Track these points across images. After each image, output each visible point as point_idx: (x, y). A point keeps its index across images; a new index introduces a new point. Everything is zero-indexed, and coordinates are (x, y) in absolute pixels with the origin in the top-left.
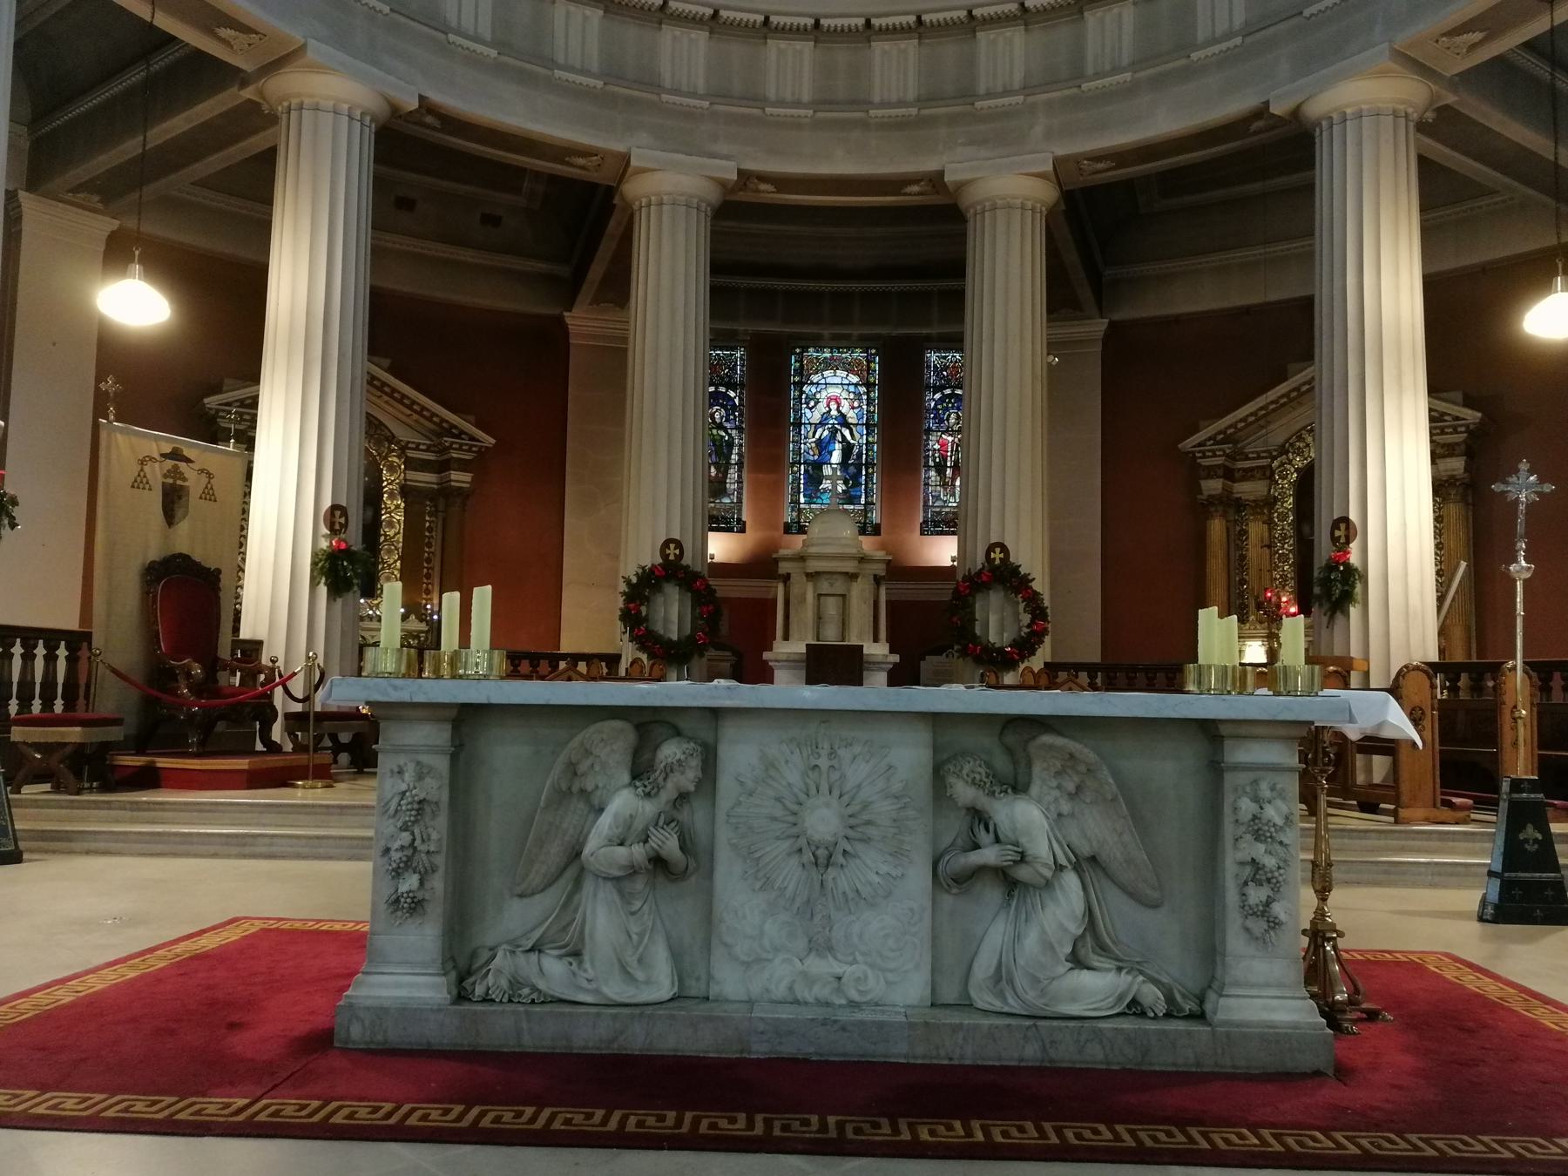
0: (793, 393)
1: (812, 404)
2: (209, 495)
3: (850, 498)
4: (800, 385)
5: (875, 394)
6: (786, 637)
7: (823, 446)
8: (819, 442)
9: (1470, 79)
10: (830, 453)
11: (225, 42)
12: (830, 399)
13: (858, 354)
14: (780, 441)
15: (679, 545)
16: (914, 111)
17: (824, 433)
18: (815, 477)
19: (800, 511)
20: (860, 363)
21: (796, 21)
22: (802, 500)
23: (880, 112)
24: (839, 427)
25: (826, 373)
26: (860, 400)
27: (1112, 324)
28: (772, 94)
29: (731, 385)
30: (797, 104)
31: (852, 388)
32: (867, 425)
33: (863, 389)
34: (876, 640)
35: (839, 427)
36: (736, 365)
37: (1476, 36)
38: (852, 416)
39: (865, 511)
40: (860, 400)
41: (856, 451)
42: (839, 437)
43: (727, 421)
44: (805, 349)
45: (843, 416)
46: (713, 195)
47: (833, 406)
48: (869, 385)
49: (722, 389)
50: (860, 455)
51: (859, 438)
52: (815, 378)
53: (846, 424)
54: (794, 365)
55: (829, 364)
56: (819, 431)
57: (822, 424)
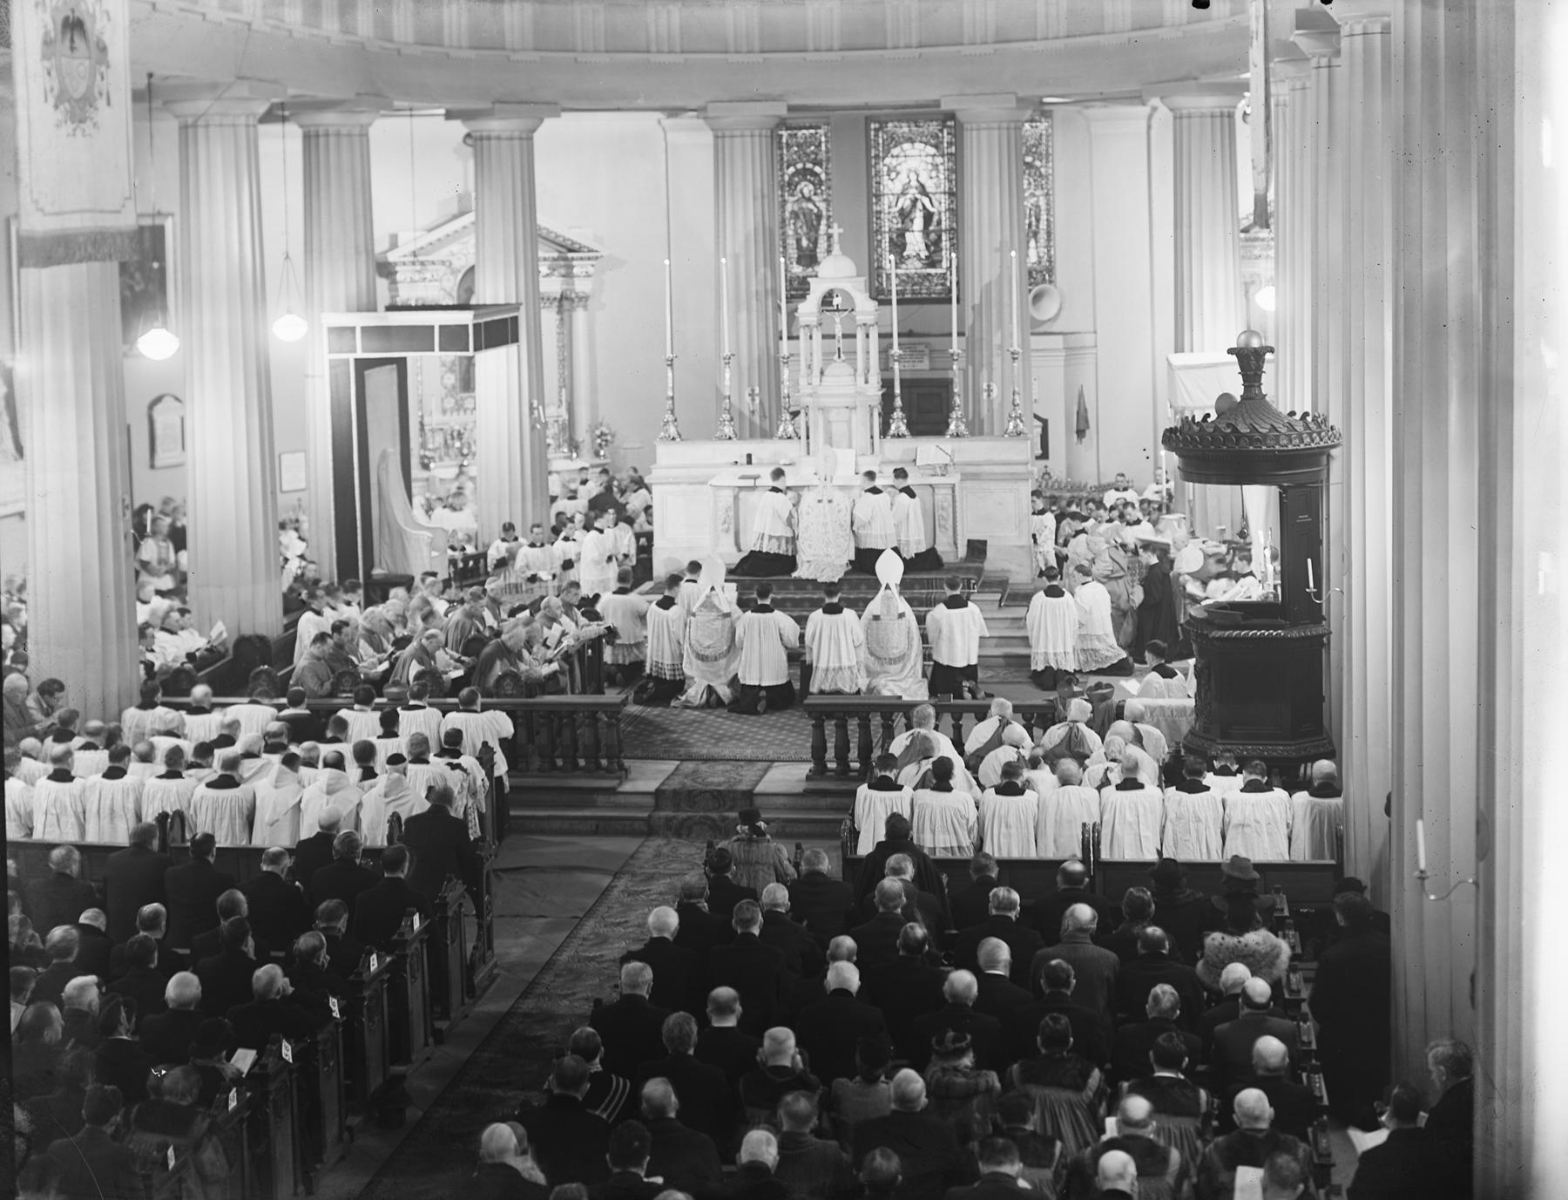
1: (893, 175)
7: (905, 215)
10: (912, 221)
17: (905, 202)
24: (918, 196)
29: (817, 163)
31: (930, 159)
35: (918, 196)
36: (820, 143)
38: (930, 187)
41: (935, 218)
42: (919, 205)
43: (815, 194)
45: (922, 186)
47: (913, 177)
49: (809, 166)
50: (939, 223)
53: (923, 190)
56: (901, 200)
57: (903, 194)
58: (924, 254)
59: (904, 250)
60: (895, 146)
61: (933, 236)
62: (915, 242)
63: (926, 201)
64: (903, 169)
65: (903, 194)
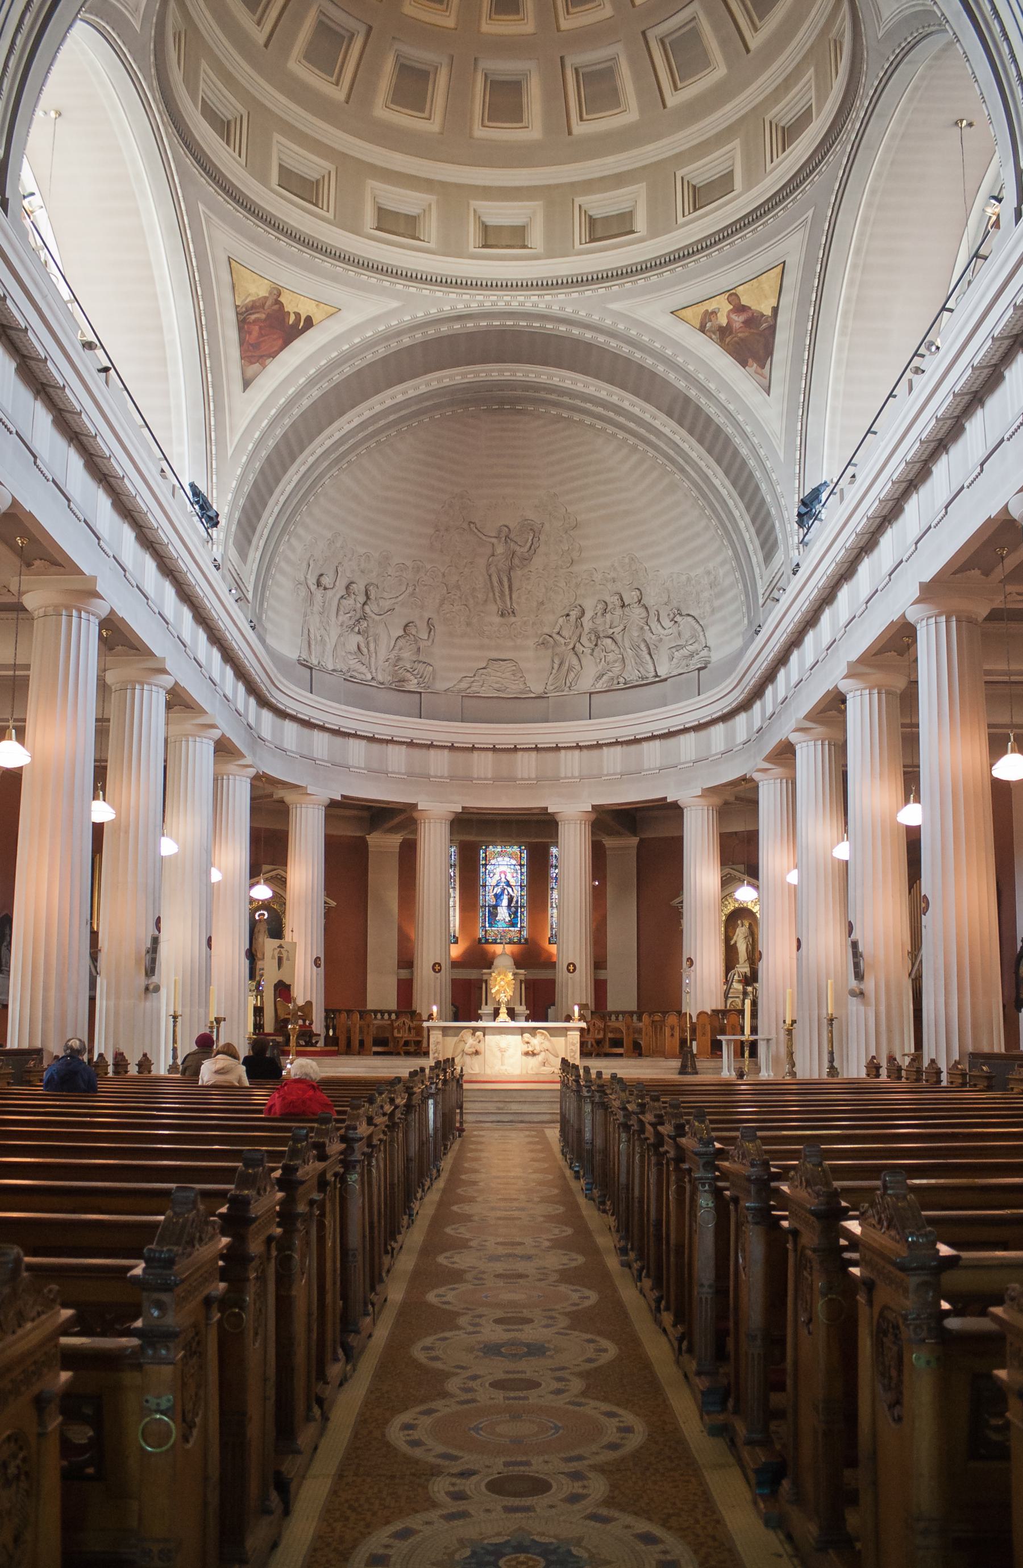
0: (482, 870)
1: (491, 875)
2: (288, 959)
3: (513, 924)
4: (486, 865)
5: (524, 870)
6: (486, 1004)
7: (498, 897)
8: (496, 895)
10: (502, 900)
12: (501, 872)
13: (516, 849)
14: (475, 896)
15: (439, 965)
17: (498, 890)
18: (493, 915)
19: (486, 931)
20: (517, 854)
22: (487, 925)
23: (521, 782)
25: (498, 859)
26: (517, 873)
27: (641, 840)
30: (486, 779)
31: (512, 867)
32: (521, 886)
33: (518, 867)
34: (521, 1005)
38: (512, 882)
39: (520, 931)
40: (517, 873)
41: (515, 899)
44: (487, 847)
45: (508, 881)
46: (451, 817)
47: (503, 876)
48: (521, 865)
50: (517, 902)
51: (516, 893)
52: (493, 862)
54: (482, 855)
55: (500, 854)
56: (496, 889)
57: (497, 885)
58: (508, 919)
59: (496, 916)
60: (494, 858)
61: (513, 909)
62: (503, 913)
63: (510, 889)
64: (498, 871)
65: (497, 885)
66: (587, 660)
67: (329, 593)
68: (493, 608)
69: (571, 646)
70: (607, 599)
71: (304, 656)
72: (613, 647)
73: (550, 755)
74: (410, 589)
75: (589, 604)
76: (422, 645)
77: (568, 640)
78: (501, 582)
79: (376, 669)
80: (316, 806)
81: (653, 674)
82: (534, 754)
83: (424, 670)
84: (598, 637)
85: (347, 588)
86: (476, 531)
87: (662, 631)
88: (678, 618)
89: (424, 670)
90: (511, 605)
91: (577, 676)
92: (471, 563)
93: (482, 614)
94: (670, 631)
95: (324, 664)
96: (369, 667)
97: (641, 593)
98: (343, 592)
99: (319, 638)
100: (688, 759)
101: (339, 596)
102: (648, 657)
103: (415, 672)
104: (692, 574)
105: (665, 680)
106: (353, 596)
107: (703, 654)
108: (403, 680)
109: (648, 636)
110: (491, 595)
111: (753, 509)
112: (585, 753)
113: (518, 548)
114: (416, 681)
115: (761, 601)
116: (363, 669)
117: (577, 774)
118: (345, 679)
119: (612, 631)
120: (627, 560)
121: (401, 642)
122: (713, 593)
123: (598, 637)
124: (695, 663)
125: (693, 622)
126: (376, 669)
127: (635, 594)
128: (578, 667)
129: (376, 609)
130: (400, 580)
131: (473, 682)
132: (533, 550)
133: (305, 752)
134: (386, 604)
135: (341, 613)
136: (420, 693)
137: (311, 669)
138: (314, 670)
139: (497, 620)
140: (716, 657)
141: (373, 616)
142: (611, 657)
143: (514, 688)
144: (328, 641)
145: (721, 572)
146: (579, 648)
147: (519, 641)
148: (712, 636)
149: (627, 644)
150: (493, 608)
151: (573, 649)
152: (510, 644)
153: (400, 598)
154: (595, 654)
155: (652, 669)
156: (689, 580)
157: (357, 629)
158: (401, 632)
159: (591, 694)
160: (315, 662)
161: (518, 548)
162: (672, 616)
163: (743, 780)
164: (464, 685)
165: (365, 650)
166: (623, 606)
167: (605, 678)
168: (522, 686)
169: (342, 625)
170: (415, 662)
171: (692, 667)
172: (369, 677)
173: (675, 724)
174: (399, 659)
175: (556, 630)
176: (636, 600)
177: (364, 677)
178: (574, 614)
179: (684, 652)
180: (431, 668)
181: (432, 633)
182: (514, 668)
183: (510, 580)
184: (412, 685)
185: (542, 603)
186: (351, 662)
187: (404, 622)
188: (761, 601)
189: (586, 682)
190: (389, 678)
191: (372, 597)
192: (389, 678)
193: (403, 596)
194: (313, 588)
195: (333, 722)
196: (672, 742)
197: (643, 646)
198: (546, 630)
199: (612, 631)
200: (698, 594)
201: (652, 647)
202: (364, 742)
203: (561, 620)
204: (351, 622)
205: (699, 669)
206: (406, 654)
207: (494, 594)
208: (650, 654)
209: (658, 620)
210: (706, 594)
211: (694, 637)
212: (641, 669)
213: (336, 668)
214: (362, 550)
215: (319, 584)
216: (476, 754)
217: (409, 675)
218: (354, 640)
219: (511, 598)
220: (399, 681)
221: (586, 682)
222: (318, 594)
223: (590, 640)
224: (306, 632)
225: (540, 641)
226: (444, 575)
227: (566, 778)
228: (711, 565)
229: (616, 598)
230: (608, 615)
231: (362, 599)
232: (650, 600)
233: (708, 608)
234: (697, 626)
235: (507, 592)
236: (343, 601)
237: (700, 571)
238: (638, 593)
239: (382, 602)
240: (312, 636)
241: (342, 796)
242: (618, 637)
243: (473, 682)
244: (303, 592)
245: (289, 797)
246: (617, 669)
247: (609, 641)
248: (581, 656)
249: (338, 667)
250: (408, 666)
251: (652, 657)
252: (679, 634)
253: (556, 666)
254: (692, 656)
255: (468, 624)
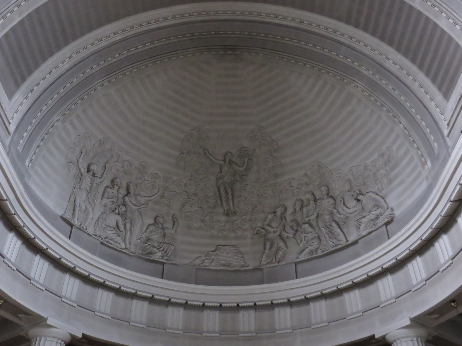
9: (439, 326)
11: (20, 319)
16: (254, 334)
21: (213, 304)
23: (243, 335)
28: (205, 329)
30: (214, 332)
37: (436, 316)
66: (292, 243)
67: (97, 180)
68: (220, 210)
69: (278, 233)
70: (303, 197)
71: (68, 216)
72: (310, 229)
73: (266, 314)
74: (161, 193)
75: (289, 204)
76: (167, 231)
77: (276, 229)
78: (227, 193)
79: (130, 243)
80: (55, 340)
81: (345, 240)
82: (252, 313)
83: (168, 249)
84: (298, 225)
85: (112, 181)
86: (209, 155)
87: (348, 211)
88: (360, 197)
89: (168, 249)
90: (234, 207)
91: (285, 254)
92: (205, 178)
93: (213, 214)
94: (355, 209)
95: (85, 228)
96: (124, 242)
97: (328, 188)
98: (107, 183)
99: (84, 208)
100: (389, 296)
101: (105, 185)
102: (339, 230)
103: (161, 249)
104: (369, 162)
105: (355, 243)
106: (116, 188)
107: (389, 212)
108: (151, 253)
109: (337, 217)
110: (219, 202)
111: (426, 66)
112: (296, 310)
113: (237, 168)
114: (160, 254)
115: (446, 132)
116: (118, 239)
117: (289, 325)
118: (102, 243)
119: (308, 219)
120: (316, 167)
121: (151, 228)
122: (388, 169)
123: (298, 225)
124: (383, 220)
125: (374, 196)
126: (130, 243)
127: (324, 189)
128: (284, 247)
129: (134, 202)
130: (153, 185)
131: (205, 260)
132: (247, 169)
133: (53, 288)
134: (142, 200)
135: (105, 196)
136: (163, 264)
137: (72, 225)
138: (74, 228)
139: (223, 218)
140: (397, 213)
141: (131, 205)
142: (310, 236)
143: (236, 263)
144: (91, 210)
145: (394, 148)
146: (285, 235)
147: (239, 233)
148: (392, 201)
149: (321, 225)
150: (220, 210)
151: (280, 235)
152: (233, 235)
153: (152, 198)
154: (297, 237)
155: (343, 238)
156: (366, 167)
157: (117, 211)
158: (152, 221)
159: (296, 264)
160: (76, 222)
161: (237, 168)
162: (355, 195)
163: (453, 301)
164: (198, 262)
165: (122, 228)
166: (315, 200)
167: (307, 251)
168: (243, 264)
169: (105, 206)
170: (161, 243)
171: (380, 224)
172: (123, 246)
173: (374, 268)
174: (148, 239)
175: (267, 222)
176: (325, 192)
177: (119, 245)
178: (279, 212)
179: (372, 216)
180: (173, 247)
181: (176, 224)
182: (236, 251)
183: (232, 191)
184: (158, 256)
185: (256, 206)
186: (110, 232)
187: (154, 214)
188: (446, 132)
189: (292, 257)
190: (140, 251)
191: (132, 191)
192: (140, 251)
193: (154, 197)
194: (84, 171)
195: (83, 268)
196: (371, 288)
197: (334, 224)
198: (259, 224)
199: (308, 219)
200: (375, 174)
201: (341, 224)
202: (111, 295)
203: (270, 216)
204: (113, 206)
205: (387, 224)
206: (155, 237)
207: (221, 200)
208: (340, 227)
209: (344, 204)
210: (383, 171)
211: (377, 206)
212: (334, 241)
213: (96, 234)
214: (126, 158)
215: (89, 170)
216: (206, 313)
217: (155, 249)
218: (113, 219)
219: (233, 202)
220: (148, 254)
221: (292, 257)
222: (87, 179)
223: (292, 227)
224: (72, 199)
225: (256, 231)
226: (185, 185)
227: (280, 329)
228: (384, 148)
229: (309, 195)
230: (305, 210)
231: (123, 192)
232: (336, 193)
233: (385, 181)
234: (377, 197)
235: (230, 197)
236: (109, 190)
237: (375, 156)
238: (326, 188)
239: (139, 198)
240: (78, 204)
241: (83, 334)
242: (314, 223)
243: (205, 260)
244: (74, 171)
245: (32, 332)
246: (315, 244)
247: (307, 226)
248: (287, 240)
249: (98, 233)
250: (156, 245)
251: (342, 230)
252: (363, 209)
253: (268, 246)
254: (377, 218)
255: (203, 221)
